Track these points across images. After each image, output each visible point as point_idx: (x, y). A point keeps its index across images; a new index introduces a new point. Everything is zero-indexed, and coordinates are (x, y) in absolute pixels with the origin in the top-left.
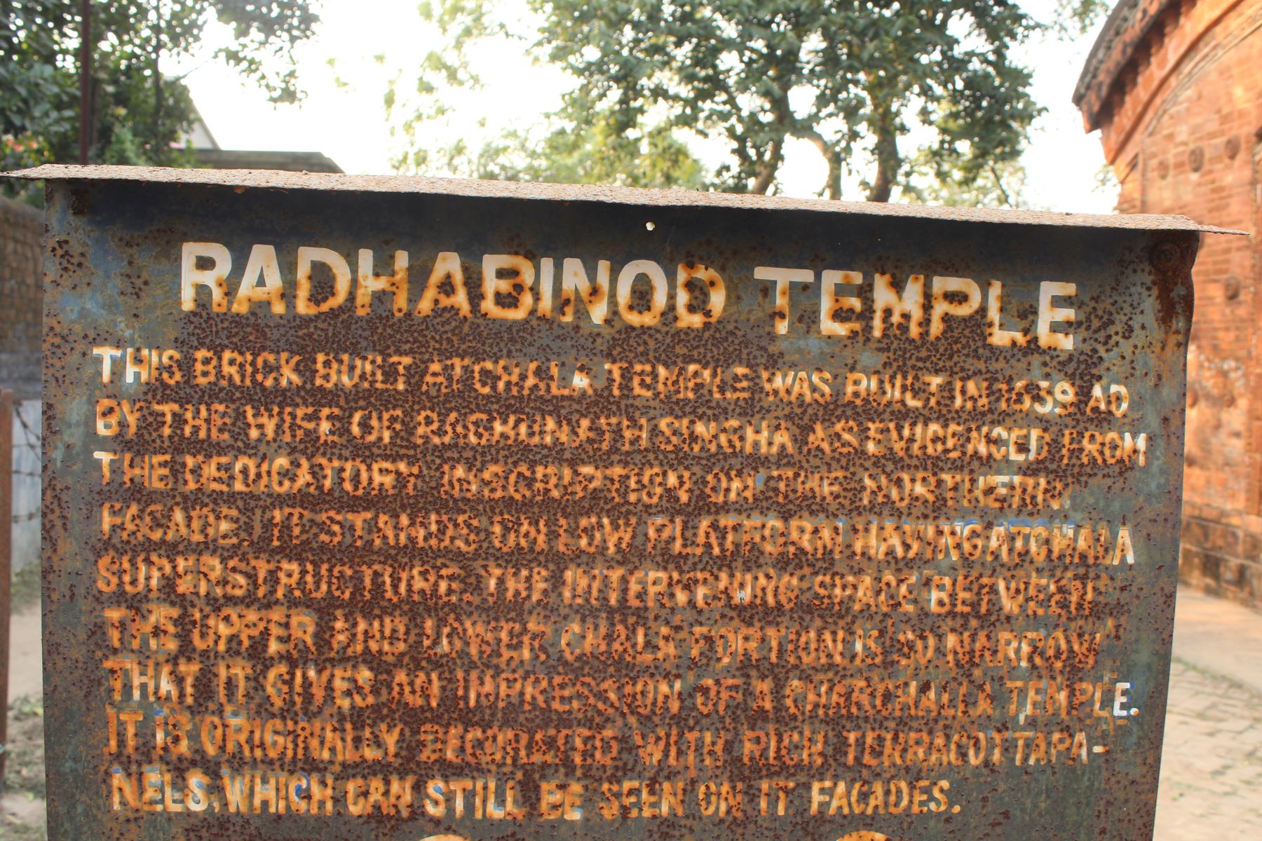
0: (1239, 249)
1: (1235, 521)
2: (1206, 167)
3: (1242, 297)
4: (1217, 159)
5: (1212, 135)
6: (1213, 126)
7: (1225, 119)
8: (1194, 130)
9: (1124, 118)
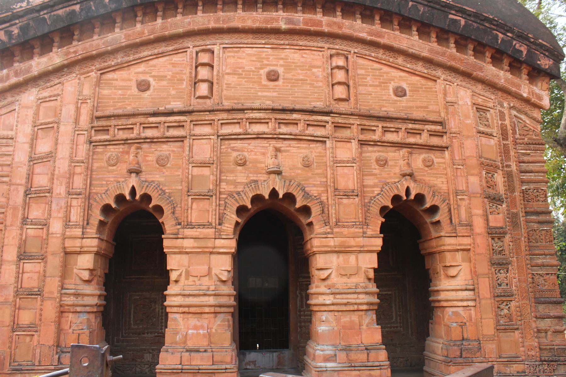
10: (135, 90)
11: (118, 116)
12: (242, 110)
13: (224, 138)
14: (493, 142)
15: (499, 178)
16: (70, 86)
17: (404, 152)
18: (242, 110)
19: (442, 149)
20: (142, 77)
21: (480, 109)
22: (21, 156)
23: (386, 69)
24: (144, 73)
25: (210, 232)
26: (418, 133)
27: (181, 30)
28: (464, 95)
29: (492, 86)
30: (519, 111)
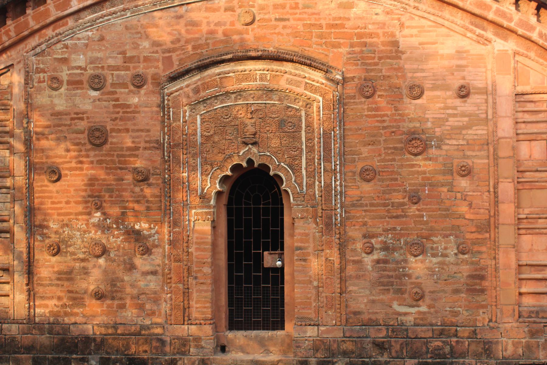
0: (145, 148)
1: (159, 331)
2: (108, 88)
3: (151, 181)
4: (124, 85)
5: (117, 68)
7: (128, 60)
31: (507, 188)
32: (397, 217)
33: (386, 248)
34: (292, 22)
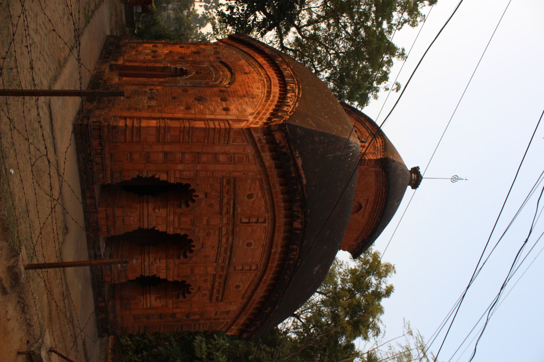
5: (223, 56)
6: (225, 56)
8: (225, 53)
9: (230, 42)
10: (248, 193)
11: (235, 188)
12: (233, 235)
13: (220, 229)
14: (213, 316)
15: (197, 317)
16: (254, 168)
17: (210, 287)
18: (233, 235)
19: (211, 299)
20: (255, 196)
21: (228, 312)
22: (217, 149)
23: (249, 283)
24: (257, 196)
25: (177, 226)
26: (218, 291)
27: (276, 213)
28: (234, 308)
29: (238, 317)
30: (226, 325)
31: (180, 115)
32: (166, 95)
33: (151, 93)
34: (248, 80)
